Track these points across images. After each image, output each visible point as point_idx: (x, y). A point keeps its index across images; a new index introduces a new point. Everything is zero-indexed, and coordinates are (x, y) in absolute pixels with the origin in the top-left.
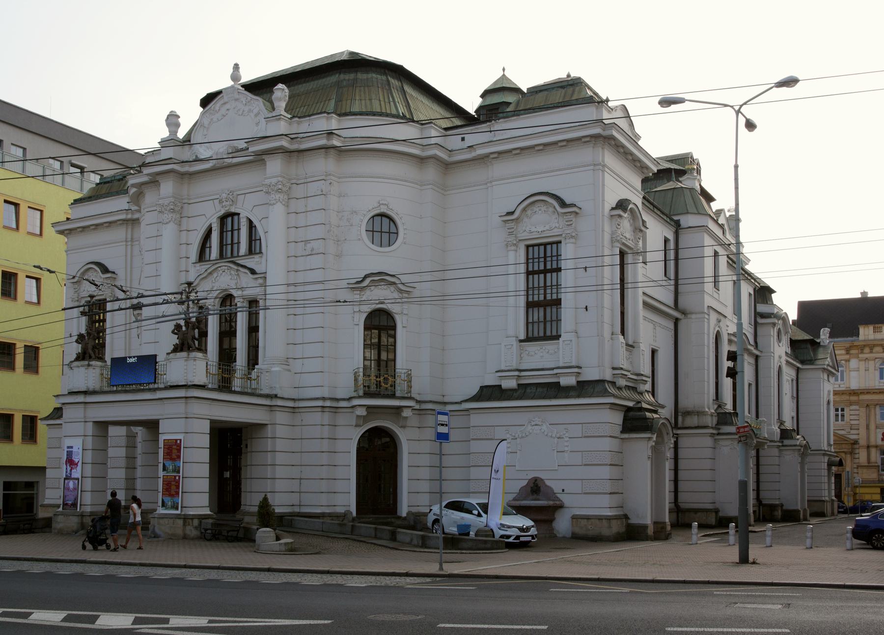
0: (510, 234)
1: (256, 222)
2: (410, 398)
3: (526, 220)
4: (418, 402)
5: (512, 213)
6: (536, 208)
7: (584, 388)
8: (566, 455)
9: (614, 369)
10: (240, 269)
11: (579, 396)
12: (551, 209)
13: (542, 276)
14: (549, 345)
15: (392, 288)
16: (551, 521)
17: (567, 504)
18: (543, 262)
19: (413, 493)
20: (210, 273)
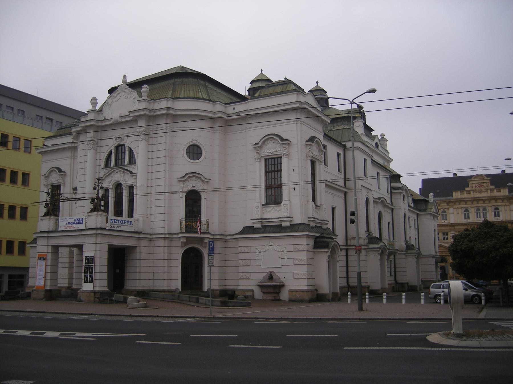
0: (257, 153)
1: (133, 149)
2: (208, 233)
3: (264, 147)
4: (212, 235)
7: (293, 227)
8: (286, 260)
9: (309, 218)
10: (125, 171)
11: (291, 232)
13: (273, 173)
14: (276, 208)
15: (199, 180)
16: (278, 293)
18: (273, 167)
19: (211, 279)
20: (111, 174)
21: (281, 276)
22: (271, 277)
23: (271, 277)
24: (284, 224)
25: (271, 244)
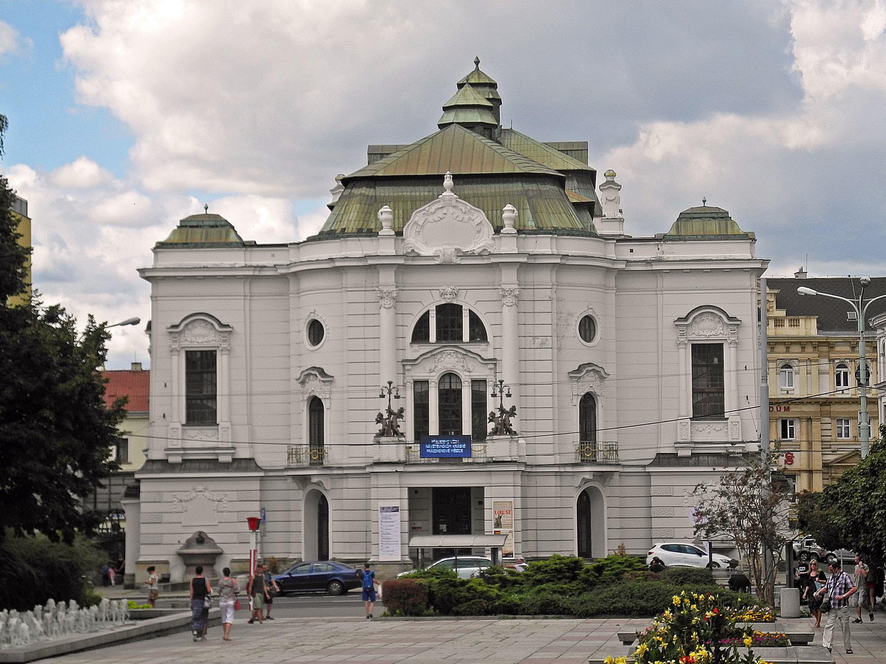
3: (187, 331)
5: (177, 326)
6: (196, 324)
12: (210, 326)
17: (225, 551)
21: (216, 538)
22: (201, 539)
23: (201, 539)
24: (222, 459)
25: (200, 488)
